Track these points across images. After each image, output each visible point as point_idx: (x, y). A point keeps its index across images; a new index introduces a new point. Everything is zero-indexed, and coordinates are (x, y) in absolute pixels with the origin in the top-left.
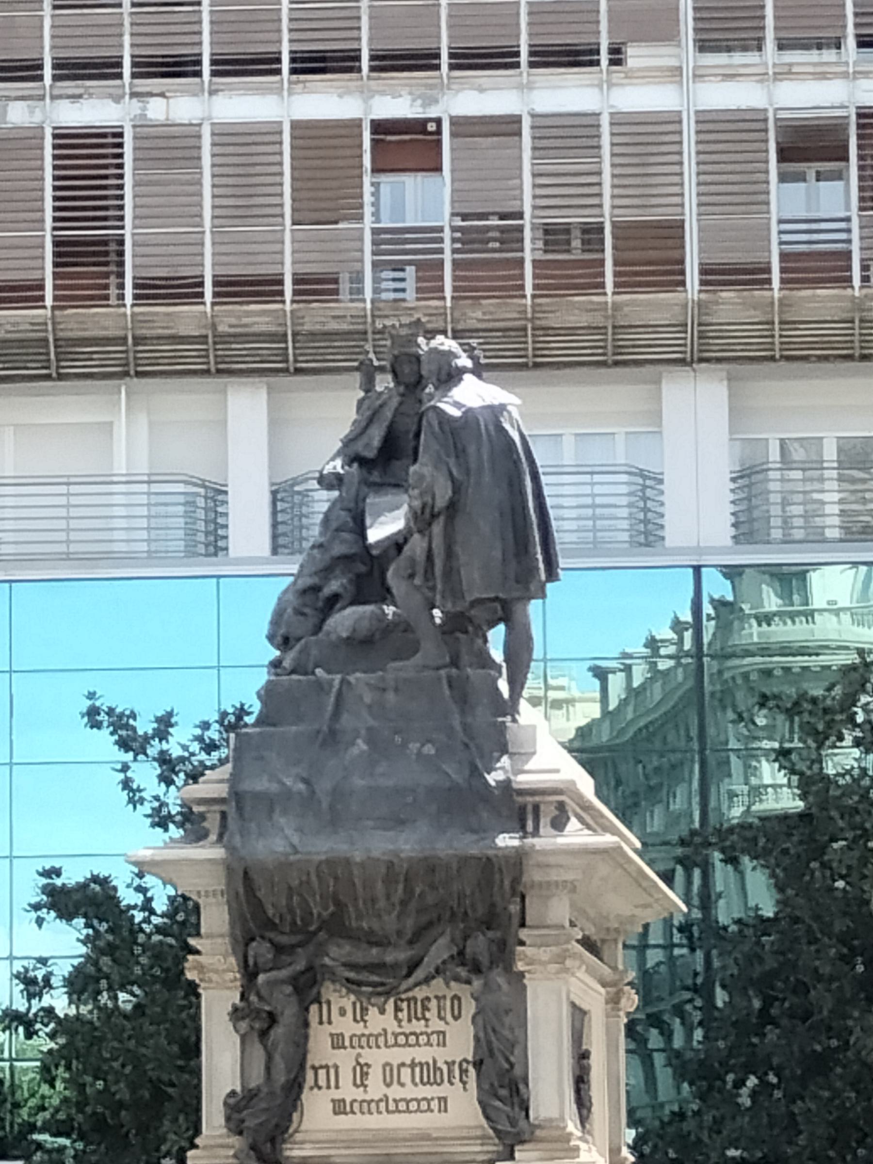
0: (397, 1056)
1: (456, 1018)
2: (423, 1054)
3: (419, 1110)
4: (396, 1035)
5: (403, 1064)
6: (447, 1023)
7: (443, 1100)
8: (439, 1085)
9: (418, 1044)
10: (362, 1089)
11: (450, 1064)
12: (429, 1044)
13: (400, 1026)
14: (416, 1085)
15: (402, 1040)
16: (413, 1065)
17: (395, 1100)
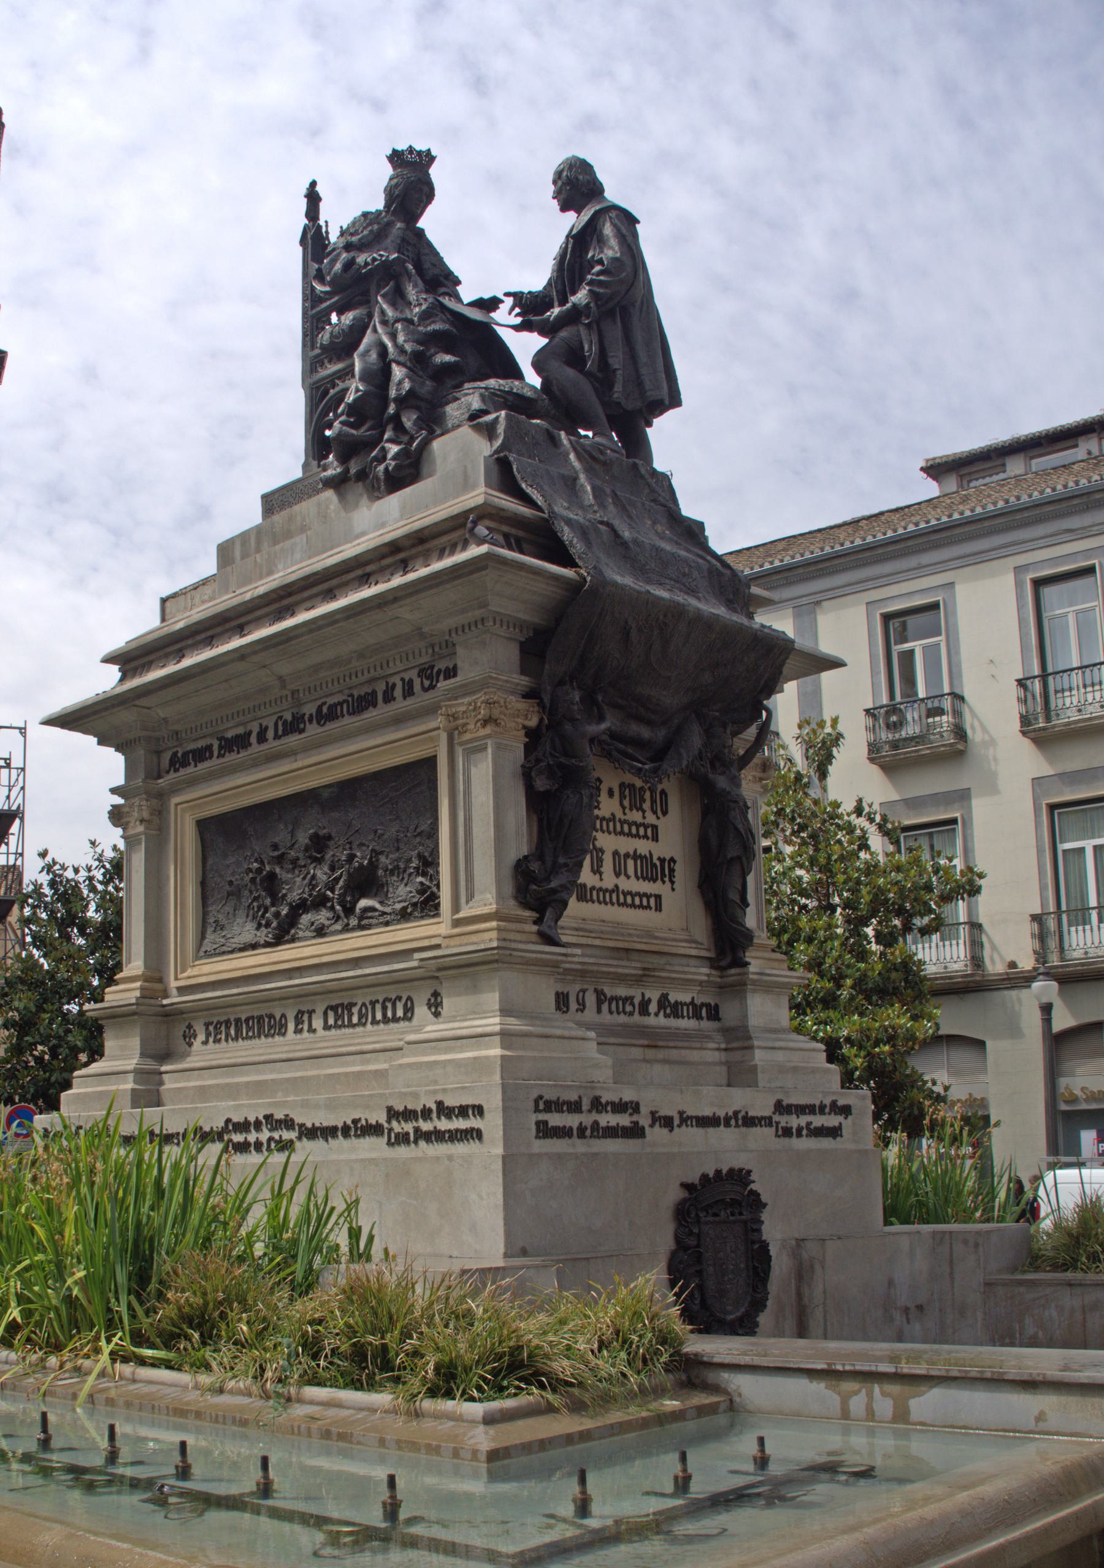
0: (626, 845)
1: (665, 813)
2: (643, 847)
3: (641, 906)
4: (622, 822)
5: (627, 855)
6: (658, 818)
7: (658, 897)
8: (655, 881)
9: (637, 836)
10: (598, 876)
11: (662, 860)
12: (646, 837)
13: (625, 814)
14: (638, 878)
15: (626, 828)
16: (636, 856)
17: (623, 892)
